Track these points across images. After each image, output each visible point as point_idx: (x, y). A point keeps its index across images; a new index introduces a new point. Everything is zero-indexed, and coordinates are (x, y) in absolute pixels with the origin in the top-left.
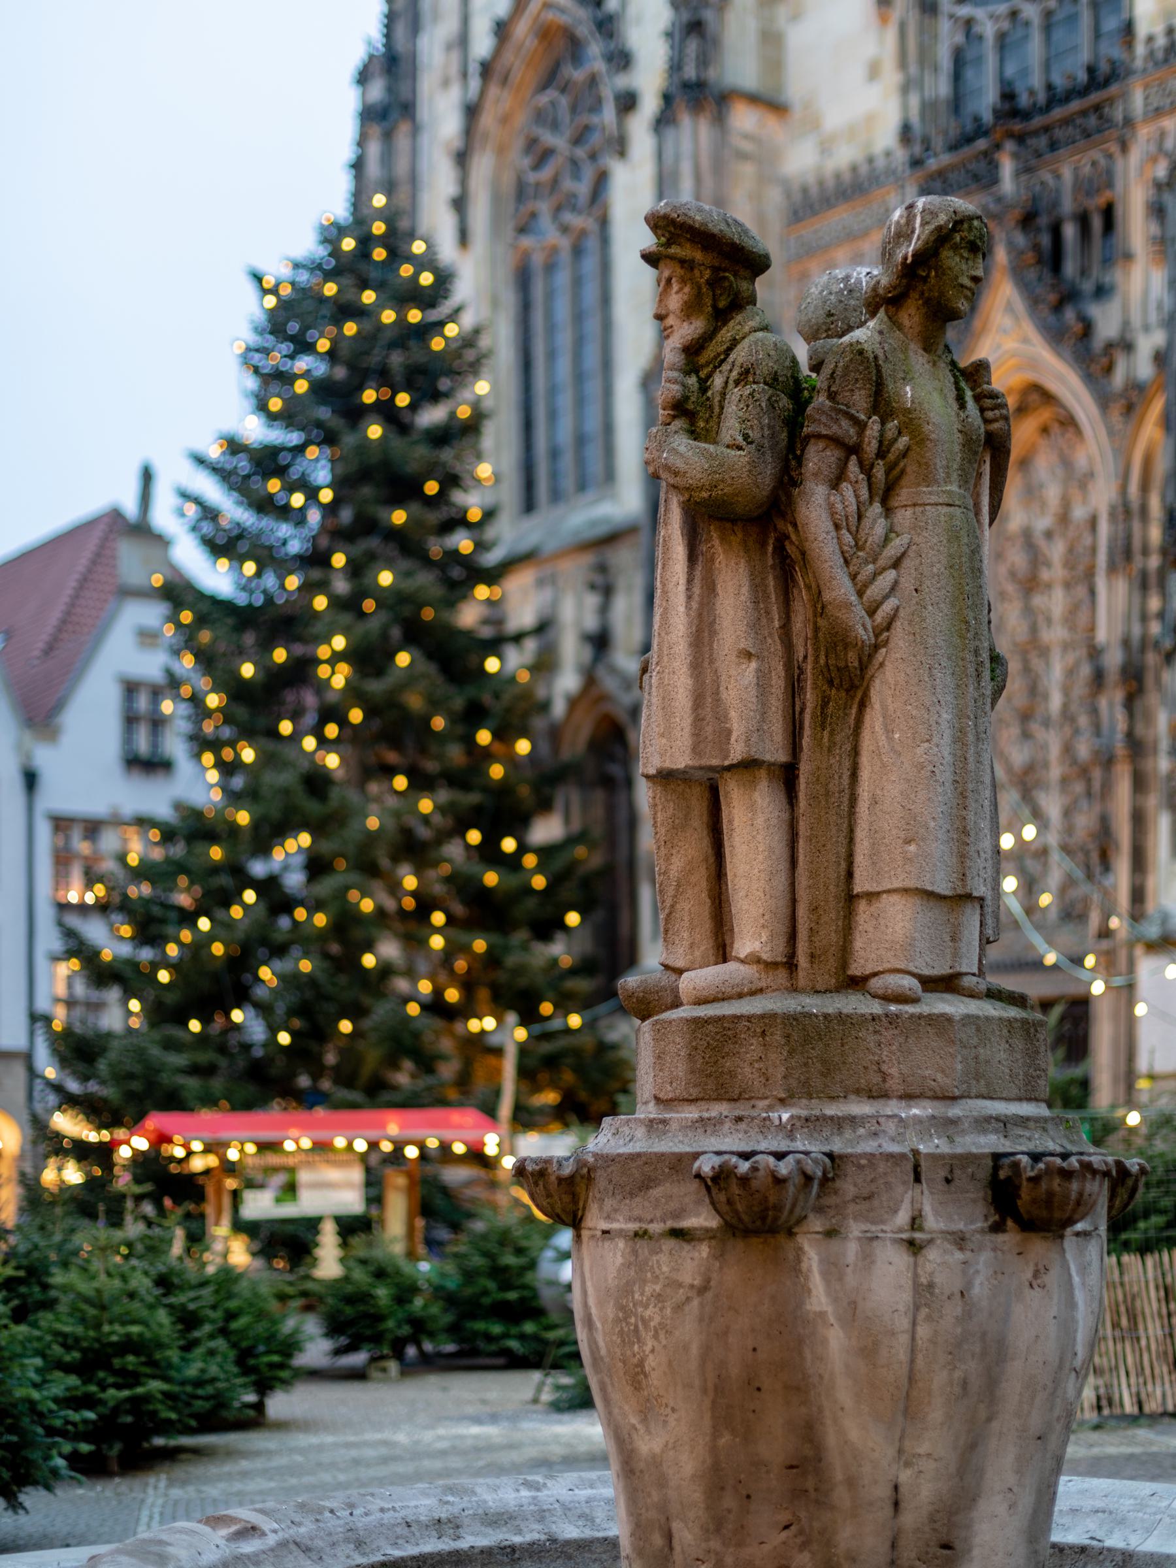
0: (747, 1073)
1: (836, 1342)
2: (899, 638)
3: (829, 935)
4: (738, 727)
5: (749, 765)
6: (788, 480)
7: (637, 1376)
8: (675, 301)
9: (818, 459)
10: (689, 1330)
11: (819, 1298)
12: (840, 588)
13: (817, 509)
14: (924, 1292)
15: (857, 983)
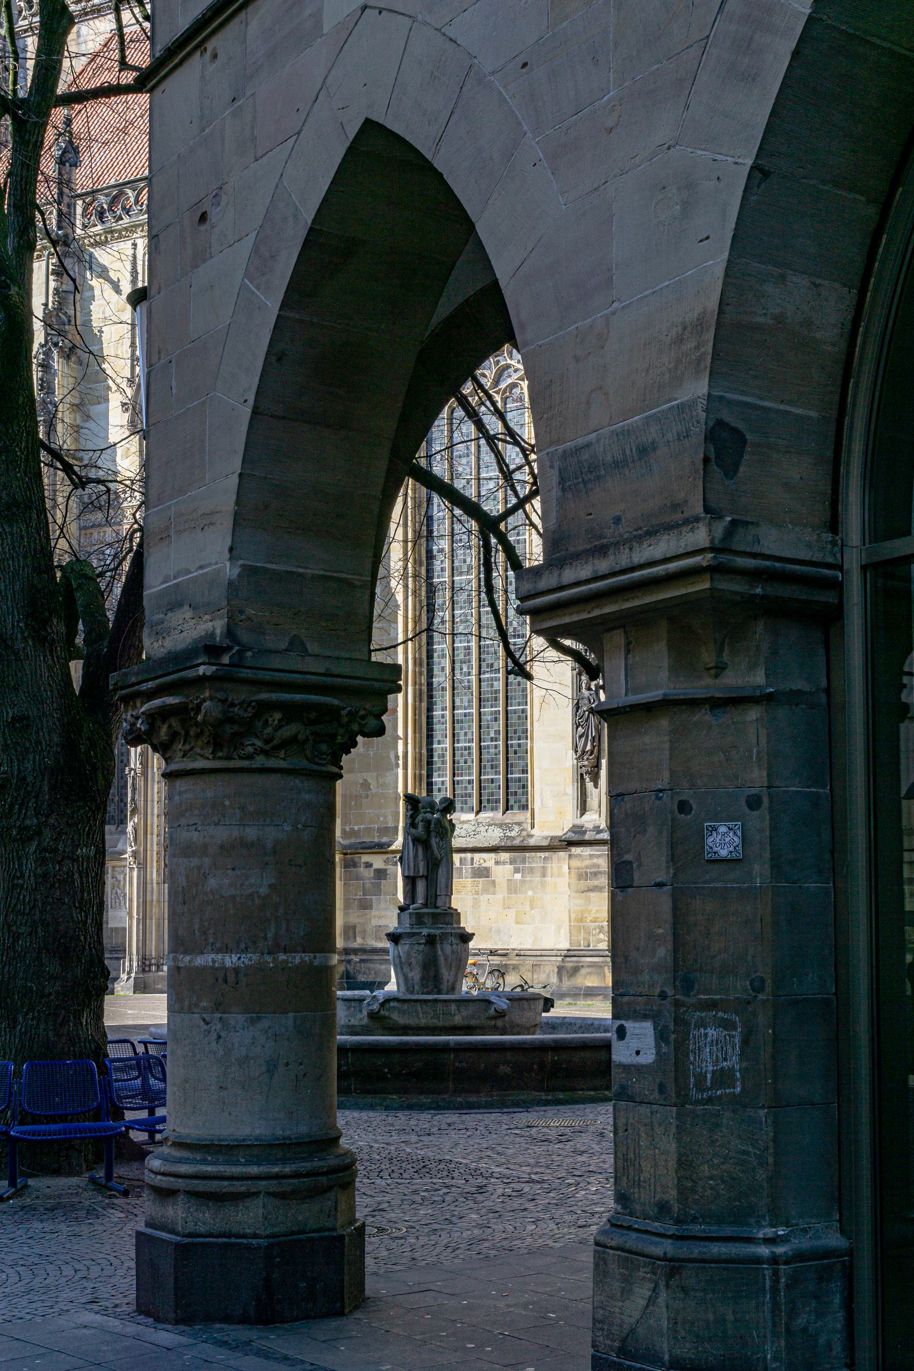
0: (426, 921)
1: (442, 959)
2: (444, 860)
3: (433, 901)
4: (421, 871)
5: (422, 876)
6: (429, 835)
7: (410, 964)
8: (409, 807)
9: (433, 834)
10: (420, 957)
11: (440, 953)
12: (436, 852)
13: (434, 841)
14: (453, 952)
15: (437, 908)
